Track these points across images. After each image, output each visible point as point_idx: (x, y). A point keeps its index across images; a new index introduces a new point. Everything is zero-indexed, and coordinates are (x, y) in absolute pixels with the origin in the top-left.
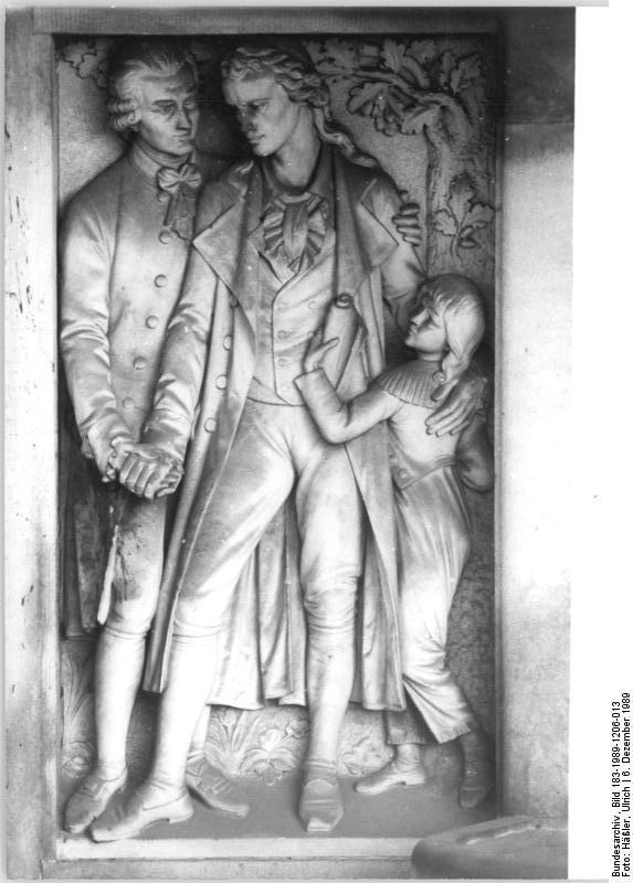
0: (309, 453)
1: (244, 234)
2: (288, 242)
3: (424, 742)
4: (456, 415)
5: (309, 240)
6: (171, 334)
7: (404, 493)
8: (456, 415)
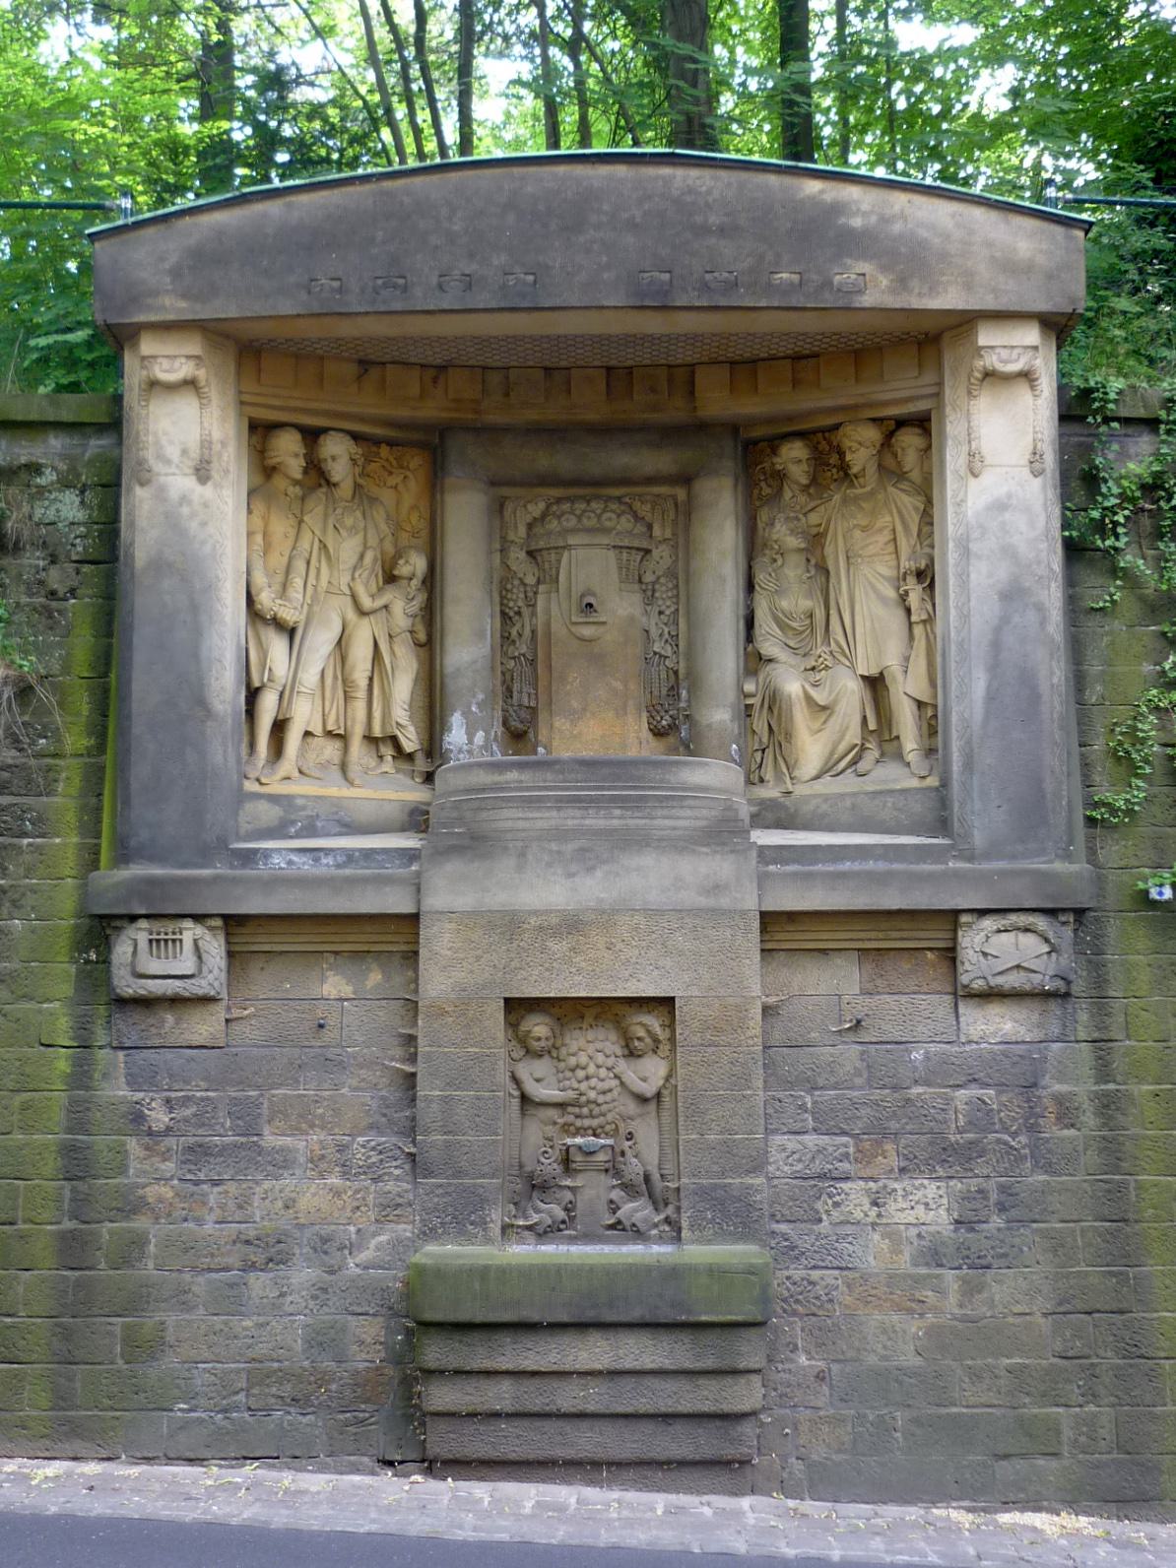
0: (351, 615)
1: (326, 516)
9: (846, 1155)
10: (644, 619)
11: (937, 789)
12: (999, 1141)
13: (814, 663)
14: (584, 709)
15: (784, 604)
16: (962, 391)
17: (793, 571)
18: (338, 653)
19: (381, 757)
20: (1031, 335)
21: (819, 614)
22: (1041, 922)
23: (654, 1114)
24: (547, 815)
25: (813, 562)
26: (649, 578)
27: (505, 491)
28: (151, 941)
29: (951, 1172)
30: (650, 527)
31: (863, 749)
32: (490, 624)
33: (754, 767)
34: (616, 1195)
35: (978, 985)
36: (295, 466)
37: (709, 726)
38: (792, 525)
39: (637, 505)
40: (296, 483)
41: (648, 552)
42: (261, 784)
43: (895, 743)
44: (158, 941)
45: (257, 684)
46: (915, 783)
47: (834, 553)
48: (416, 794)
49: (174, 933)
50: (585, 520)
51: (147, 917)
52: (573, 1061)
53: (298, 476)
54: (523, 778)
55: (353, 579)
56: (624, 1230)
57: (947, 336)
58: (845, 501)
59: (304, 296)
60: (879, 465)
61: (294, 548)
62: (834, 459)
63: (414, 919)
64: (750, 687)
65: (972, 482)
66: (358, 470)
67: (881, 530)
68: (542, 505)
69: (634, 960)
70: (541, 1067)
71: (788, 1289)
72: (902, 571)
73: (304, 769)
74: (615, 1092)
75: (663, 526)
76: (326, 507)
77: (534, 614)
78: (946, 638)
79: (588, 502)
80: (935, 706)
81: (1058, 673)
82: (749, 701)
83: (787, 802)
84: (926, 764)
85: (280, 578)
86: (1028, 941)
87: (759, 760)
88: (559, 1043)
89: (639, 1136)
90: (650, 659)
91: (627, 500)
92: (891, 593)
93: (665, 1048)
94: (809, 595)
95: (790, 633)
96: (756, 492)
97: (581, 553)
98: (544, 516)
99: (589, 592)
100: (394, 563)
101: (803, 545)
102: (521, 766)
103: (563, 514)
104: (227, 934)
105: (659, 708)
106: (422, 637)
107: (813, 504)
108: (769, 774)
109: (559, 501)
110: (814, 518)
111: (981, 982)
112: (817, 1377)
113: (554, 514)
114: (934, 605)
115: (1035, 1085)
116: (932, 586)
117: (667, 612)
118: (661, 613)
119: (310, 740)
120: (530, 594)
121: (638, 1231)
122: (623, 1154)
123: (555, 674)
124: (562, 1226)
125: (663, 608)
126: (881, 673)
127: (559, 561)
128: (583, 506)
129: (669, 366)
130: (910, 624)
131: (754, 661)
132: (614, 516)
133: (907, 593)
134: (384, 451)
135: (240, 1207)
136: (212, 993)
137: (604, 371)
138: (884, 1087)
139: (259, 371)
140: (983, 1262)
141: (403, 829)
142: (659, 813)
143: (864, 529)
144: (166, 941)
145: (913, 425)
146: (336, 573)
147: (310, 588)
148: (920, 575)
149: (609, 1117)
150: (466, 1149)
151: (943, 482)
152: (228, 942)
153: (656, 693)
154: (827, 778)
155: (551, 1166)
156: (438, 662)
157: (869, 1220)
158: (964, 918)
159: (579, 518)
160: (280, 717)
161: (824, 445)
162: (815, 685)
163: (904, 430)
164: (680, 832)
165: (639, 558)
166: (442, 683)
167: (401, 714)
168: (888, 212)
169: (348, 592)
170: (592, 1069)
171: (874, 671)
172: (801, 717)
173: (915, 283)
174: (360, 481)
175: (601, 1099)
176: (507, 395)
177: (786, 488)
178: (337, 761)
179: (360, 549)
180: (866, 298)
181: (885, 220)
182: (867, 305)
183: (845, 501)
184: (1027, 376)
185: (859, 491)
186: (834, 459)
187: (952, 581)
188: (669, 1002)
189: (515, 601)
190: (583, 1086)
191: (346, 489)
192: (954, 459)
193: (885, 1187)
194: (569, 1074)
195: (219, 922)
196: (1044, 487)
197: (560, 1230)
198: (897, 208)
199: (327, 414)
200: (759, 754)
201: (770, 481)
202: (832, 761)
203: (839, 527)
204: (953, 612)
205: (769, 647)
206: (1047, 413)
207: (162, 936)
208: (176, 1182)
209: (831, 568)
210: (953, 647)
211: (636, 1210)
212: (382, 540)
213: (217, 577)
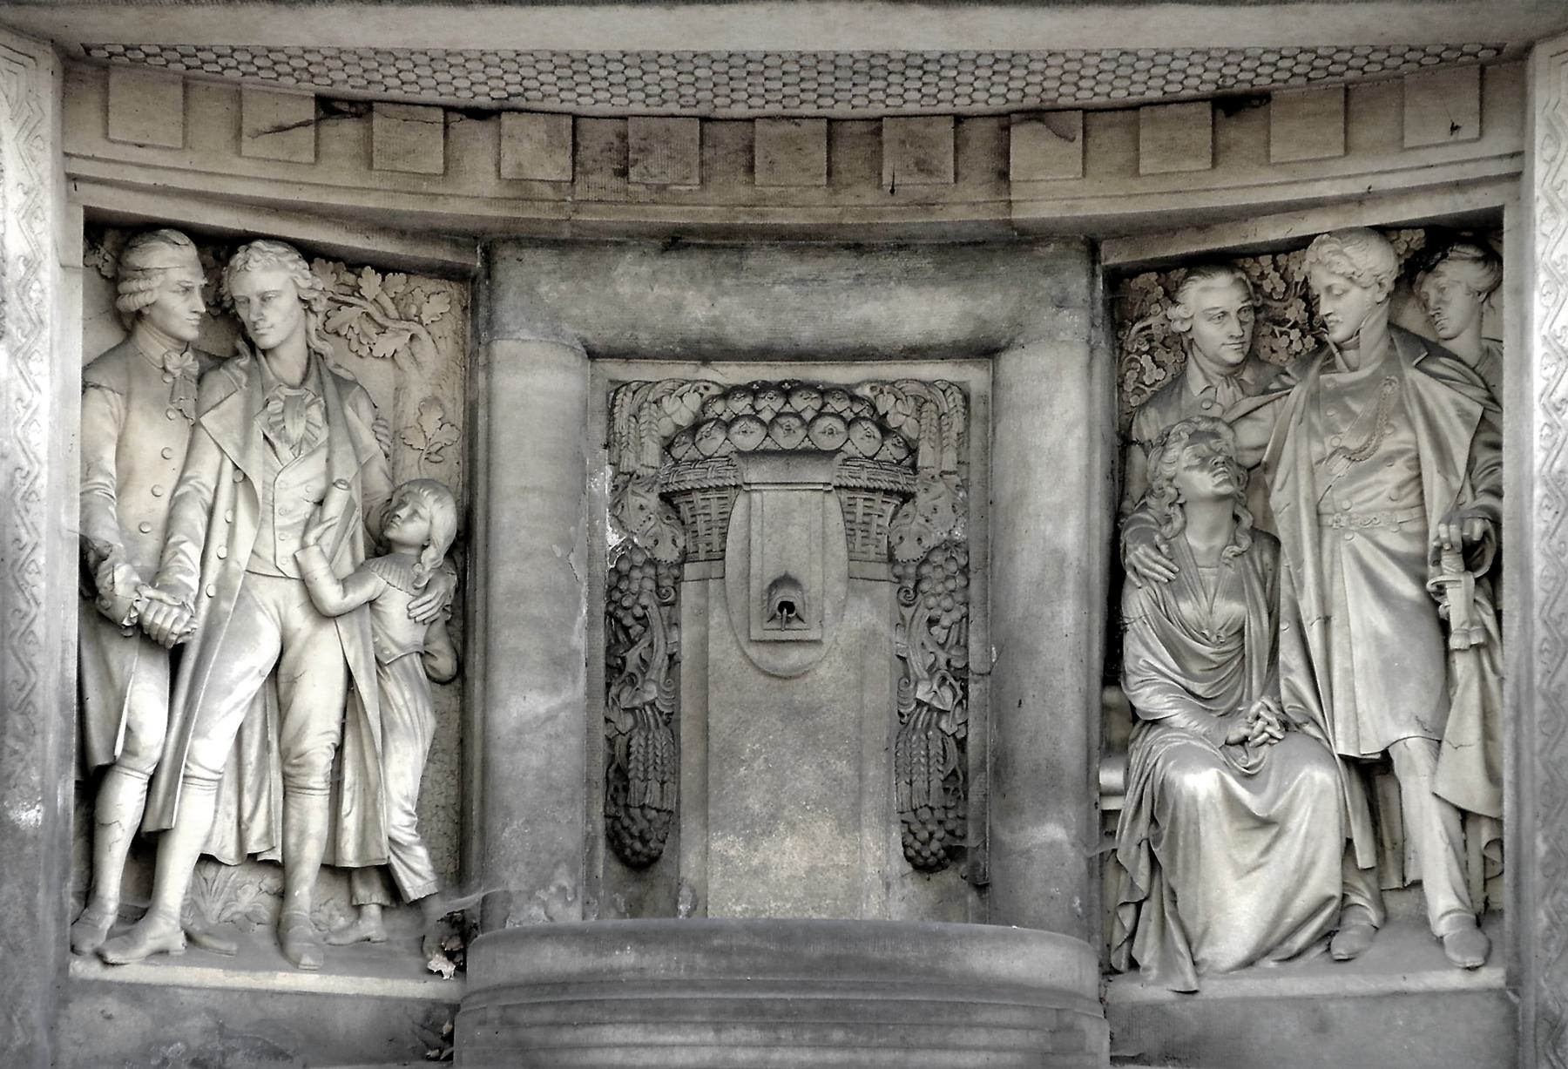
0: (300, 620)
2: (288, 425)
3: (387, 903)
4: (433, 603)
5: (306, 428)
6: (175, 502)
7: (387, 669)
8: (433, 603)
10: (898, 637)
11: (1500, 994)
13: (1244, 731)
14: (773, 817)
15: (1187, 609)
21: (1257, 628)
24: (693, 1038)
25: (1247, 521)
30: (912, 450)
31: (1345, 904)
33: (1118, 937)
37: (1026, 852)
38: (1203, 448)
39: (886, 404)
40: (185, 345)
41: (907, 497)
42: (106, 964)
43: (1413, 894)
45: (100, 759)
46: (1455, 979)
50: (778, 432)
53: (191, 333)
54: (646, 961)
55: (304, 546)
57: (1541, 53)
58: (1315, 399)
60: (1391, 325)
61: (181, 480)
66: (315, 322)
67: (1389, 459)
72: (1433, 544)
80: (1498, 822)
82: (1111, 804)
84: (1479, 940)
87: (1128, 924)
91: (866, 391)
92: (1407, 588)
94: (1235, 591)
95: (1196, 668)
96: (1131, 376)
97: (768, 500)
98: (695, 427)
101: (1226, 489)
103: (737, 418)
105: (925, 814)
107: (1247, 404)
110: (1250, 434)
113: (718, 420)
114: (1498, 615)
116: (1495, 574)
117: (946, 622)
120: (667, 582)
125: (936, 613)
126: (1385, 753)
128: (778, 404)
132: (839, 425)
133: (1441, 589)
134: (370, 282)
137: (824, 123)
139: (106, 110)
143: (1351, 456)
145: (1465, 242)
146: (267, 533)
147: (214, 566)
148: (1470, 553)
153: (920, 784)
154: (1270, 964)
156: (477, 715)
159: (768, 426)
160: (150, 827)
161: (1274, 282)
162: (1247, 777)
165: (890, 509)
166: (485, 762)
167: (399, 820)
169: (293, 573)
171: (1370, 749)
174: (317, 344)
177: (1193, 369)
179: (319, 485)
185: (1345, 378)
186: (1296, 311)
189: (639, 594)
191: (290, 363)
200: (1131, 910)
201: (1161, 355)
203: (1298, 453)
209: (1283, 537)
212: (363, 467)
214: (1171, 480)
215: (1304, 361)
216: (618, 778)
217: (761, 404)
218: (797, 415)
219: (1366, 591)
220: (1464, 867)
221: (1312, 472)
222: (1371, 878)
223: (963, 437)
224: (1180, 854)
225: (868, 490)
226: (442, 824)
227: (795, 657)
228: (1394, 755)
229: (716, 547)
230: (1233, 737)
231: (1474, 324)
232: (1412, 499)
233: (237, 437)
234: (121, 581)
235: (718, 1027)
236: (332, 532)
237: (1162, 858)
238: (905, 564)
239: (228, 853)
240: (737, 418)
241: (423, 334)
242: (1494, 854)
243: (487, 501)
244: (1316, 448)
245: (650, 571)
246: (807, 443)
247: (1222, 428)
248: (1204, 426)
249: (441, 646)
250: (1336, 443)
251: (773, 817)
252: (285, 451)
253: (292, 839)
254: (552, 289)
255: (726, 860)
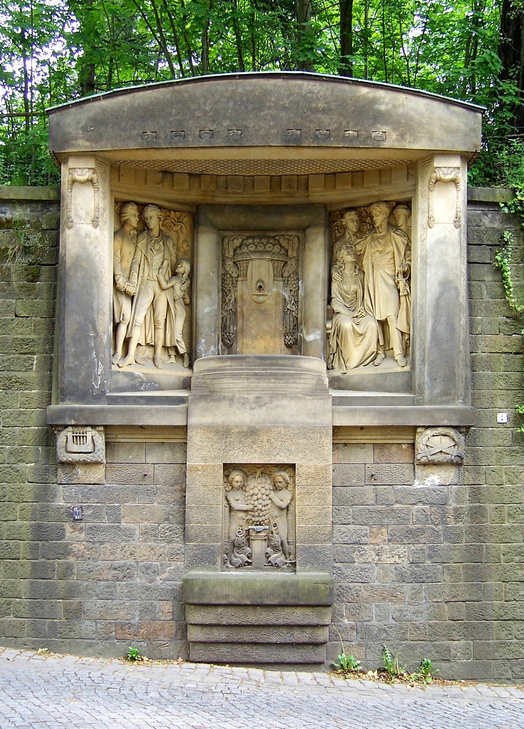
1: (147, 244)
6: (132, 264)
9: (366, 534)
12: (430, 528)
13: (357, 314)
15: (345, 287)
16: (426, 188)
17: (348, 270)
18: (151, 306)
19: (170, 356)
20: (456, 162)
22: (452, 432)
23: (285, 515)
26: (286, 274)
27: (226, 233)
28: (73, 436)
29: (410, 542)
30: (287, 251)
32: (216, 296)
34: (269, 550)
35: (424, 460)
36: (134, 221)
40: (135, 229)
42: (119, 367)
43: (391, 351)
44: (76, 437)
46: (400, 369)
47: (366, 263)
48: (187, 373)
49: (83, 433)
50: (259, 247)
51: (72, 426)
52: (251, 492)
53: (136, 226)
54: (232, 364)
55: (159, 273)
56: (272, 565)
59: (139, 139)
60: (388, 223)
62: (368, 220)
63: (184, 429)
64: (329, 325)
65: (429, 230)
66: (161, 223)
67: (388, 253)
68: (240, 240)
69: (279, 447)
70: (238, 495)
71: (341, 592)
72: (397, 272)
73: (137, 361)
74: (269, 506)
75: (293, 251)
76: (147, 240)
77: (236, 291)
78: (415, 304)
79: (261, 239)
80: (409, 335)
81: (463, 319)
83: (343, 377)
84: (405, 360)
85: (127, 273)
86: (445, 440)
88: (246, 484)
89: (279, 525)
90: (286, 312)
92: (392, 282)
93: (290, 487)
94: (356, 283)
97: (256, 263)
98: (241, 246)
99: (260, 280)
100: (175, 270)
102: (232, 359)
103: (250, 244)
104: (106, 434)
106: (188, 301)
108: (336, 365)
109: (248, 238)
111: (425, 458)
112: (351, 628)
113: (245, 244)
115: (446, 504)
116: (409, 279)
118: (291, 291)
119: (139, 347)
120: (234, 282)
121: (278, 566)
122: (272, 533)
123: (245, 318)
124: (246, 564)
126: (386, 319)
127: (247, 266)
128: (258, 241)
129: (298, 175)
130: (399, 296)
131: (331, 314)
135: (112, 554)
136: (99, 460)
138: (383, 504)
140: (421, 580)
141: (179, 389)
142: (291, 381)
143: (380, 252)
144: (80, 437)
146: (151, 271)
147: (140, 278)
149: (267, 517)
150: (206, 530)
151: (416, 230)
152: (106, 438)
155: (242, 539)
157: (375, 562)
158: (419, 430)
160: (127, 337)
163: (399, 206)
164: (299, 390)
167: (178, 336)
168: (397, 103)
169: (157, 280)
170: (259, 496)
171: (383, 318)
172: (350, 338)
173: (407, 137)
174: (163, 229)
175: (263, 509)
176: (227, 188)
178: (151, 357)
179: (162, 260)
180: (385, 143)
181: (394, 107)
182: (386, 147)
183: (372, 239)
184: (454, 182)
185: (379, 235)
187: (419, 276)
188: (293, 466)
190: (256, 503)
191: (156, 232)
192: (420, 219)
193: (382, 548)
194: (250, 498)
195: (101, 428)
196: (460, 234)
197: (245, 565)
198: (400, 101)
199: (149, 197)
202: (363, 360)
204: (419, 291)
205: (337, 306)
206: (463, 199)
207: (78, 435)
208: (85, 543)
209: (365, 271)
210: (418, 307)
211: (277, 557)
212: (171, 256)
213: (101, 271)
214: (342, 258)
215: (370, 230)
216: (224, 328)
217: (255, 241)
218: (262, 243)
219: (383, 282)
220: (402, 344)
221: (372, 256)
222: (382, 348)
223: (298, 248)
224: (343, 342)
225: (277, 260)
226: (186, 337)
227: (261, 298)
228: (388, 319)
229: (245, 273)
230: (355, 316)
231: (405, 224)
232: (393, 262)
233: (145, 248)
234: (121, 282)
235: (248, 379)
236: (165, 270)
237: (339, 344)
238: (285, 277)
239: (143, 343)
240: (250, 244)
241: (183, 226)
242: (408, 342)
243: (197, 264)
244: (373, 250)
245: (231, 279)
246: (265, 250)
247: (353, 246)
248: (349, 246)
249: (187, 296)
250: (377, 249)
251: (257, 335)
252: (155, 252)
253: (156, 340)
254: (211, 216)
255: (247, 345)
